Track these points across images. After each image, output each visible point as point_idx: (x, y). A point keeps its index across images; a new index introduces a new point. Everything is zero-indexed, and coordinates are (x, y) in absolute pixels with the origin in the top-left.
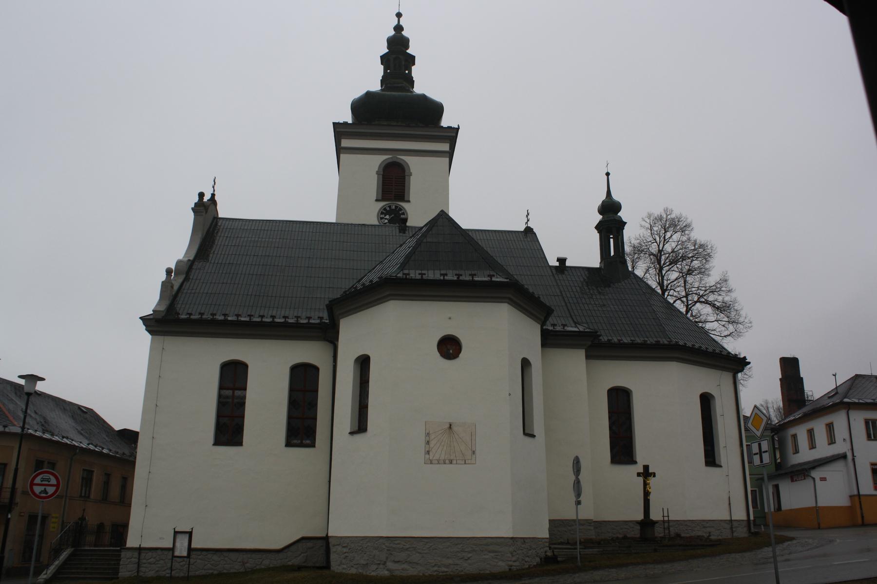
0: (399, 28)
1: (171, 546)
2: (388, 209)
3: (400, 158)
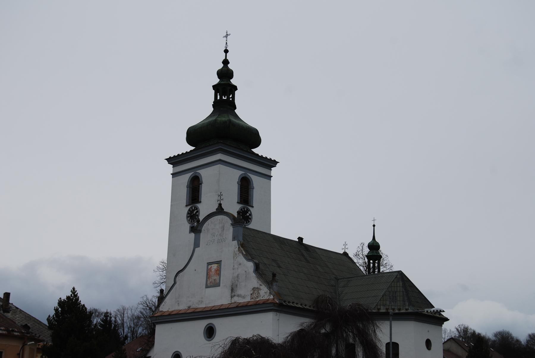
0: (226, 62)
2: (243, 210)
3: (248, 175)
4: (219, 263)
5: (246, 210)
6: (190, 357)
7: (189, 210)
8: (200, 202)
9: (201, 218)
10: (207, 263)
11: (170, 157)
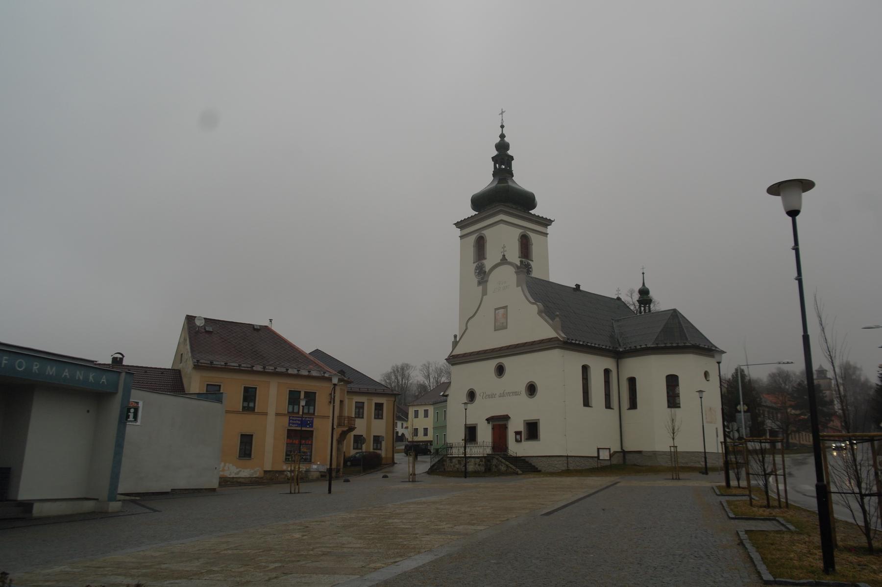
0: (502, 136)
1: (596, 455)
4: (505, 307)
5: (526, 263)
7: (477, 266)
8: (486, 259)
9: (487, 269)
11: (458, 222)
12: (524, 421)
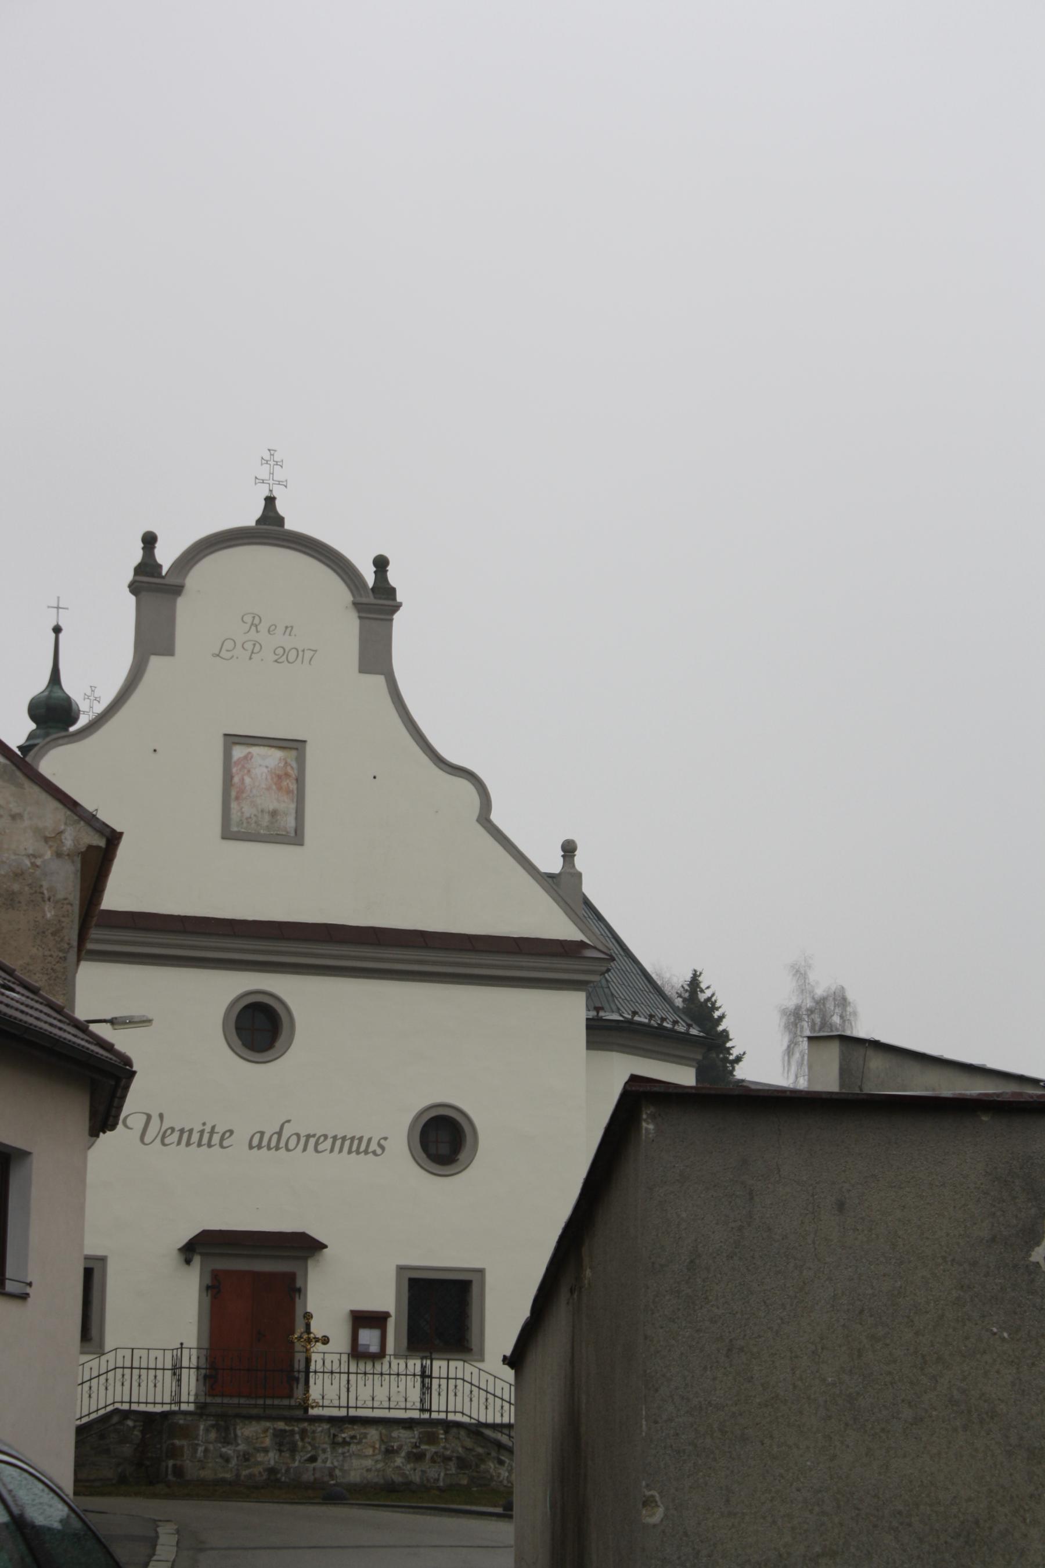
6: (149, 1117)
10: (225, 735)
12: (401, 1269)
